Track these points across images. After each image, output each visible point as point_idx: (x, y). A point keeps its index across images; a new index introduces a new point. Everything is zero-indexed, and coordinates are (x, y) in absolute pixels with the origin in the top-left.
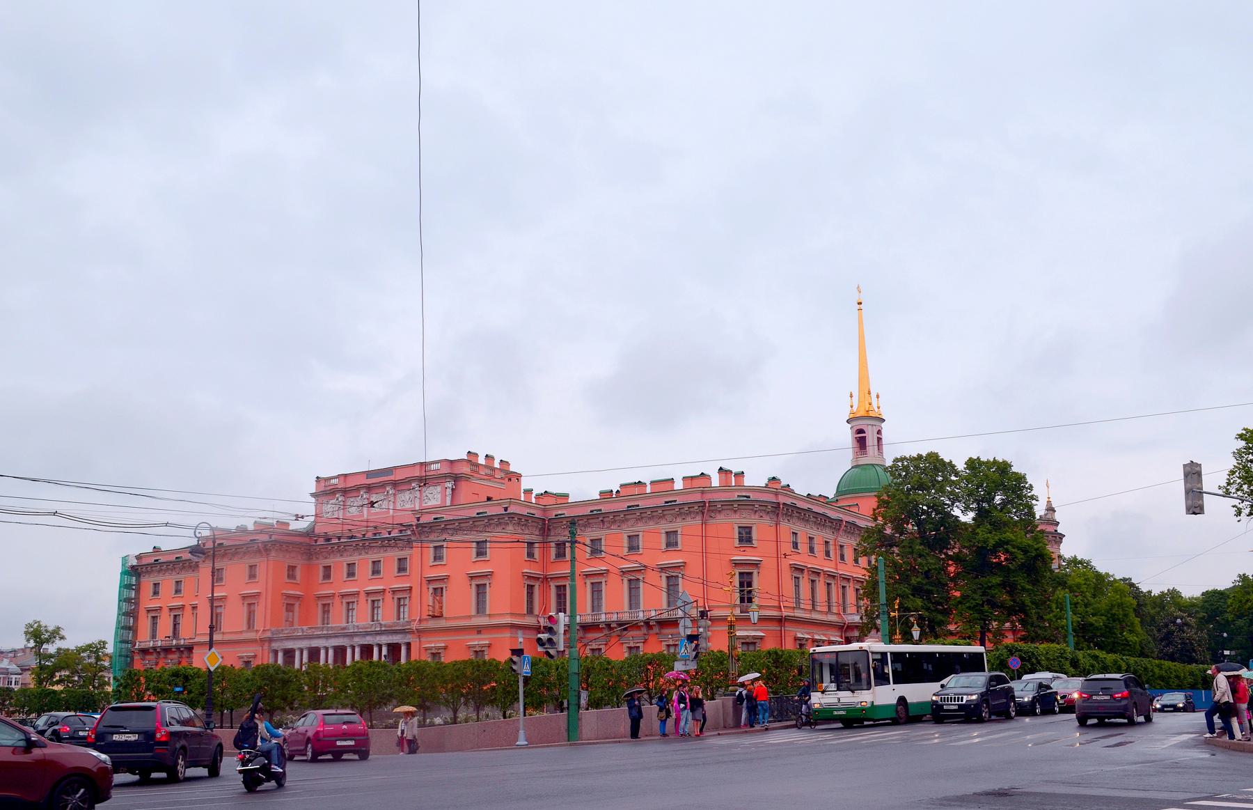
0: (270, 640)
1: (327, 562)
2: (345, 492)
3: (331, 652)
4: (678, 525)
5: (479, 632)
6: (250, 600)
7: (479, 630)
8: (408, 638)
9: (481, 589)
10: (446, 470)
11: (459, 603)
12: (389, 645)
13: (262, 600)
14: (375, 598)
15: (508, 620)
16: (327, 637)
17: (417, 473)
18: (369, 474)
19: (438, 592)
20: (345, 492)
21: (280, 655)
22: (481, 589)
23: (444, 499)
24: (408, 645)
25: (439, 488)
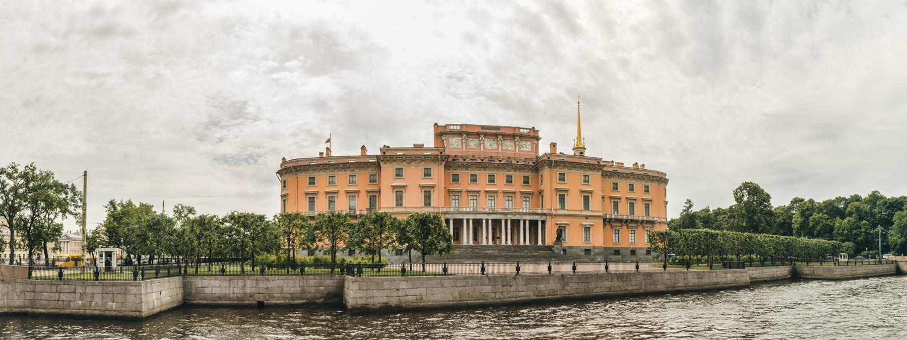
1: (456, 172)
2: (469, 134)
3: (490, 222)
7: (587, 217)
8: (544, 218)
9: (586, 199)
10: (532, 134)
11: (574, 203)
12: (530, 221)
13: (436, 189)
14: (492, 194)
15: (601, 214)
16: (488, 214)
17: (517, 132)
18: (483, 127)
20: (469, 134)
21: (451, 222)
22: (586, 199)
24: (543, 222)
25: (529, 143)
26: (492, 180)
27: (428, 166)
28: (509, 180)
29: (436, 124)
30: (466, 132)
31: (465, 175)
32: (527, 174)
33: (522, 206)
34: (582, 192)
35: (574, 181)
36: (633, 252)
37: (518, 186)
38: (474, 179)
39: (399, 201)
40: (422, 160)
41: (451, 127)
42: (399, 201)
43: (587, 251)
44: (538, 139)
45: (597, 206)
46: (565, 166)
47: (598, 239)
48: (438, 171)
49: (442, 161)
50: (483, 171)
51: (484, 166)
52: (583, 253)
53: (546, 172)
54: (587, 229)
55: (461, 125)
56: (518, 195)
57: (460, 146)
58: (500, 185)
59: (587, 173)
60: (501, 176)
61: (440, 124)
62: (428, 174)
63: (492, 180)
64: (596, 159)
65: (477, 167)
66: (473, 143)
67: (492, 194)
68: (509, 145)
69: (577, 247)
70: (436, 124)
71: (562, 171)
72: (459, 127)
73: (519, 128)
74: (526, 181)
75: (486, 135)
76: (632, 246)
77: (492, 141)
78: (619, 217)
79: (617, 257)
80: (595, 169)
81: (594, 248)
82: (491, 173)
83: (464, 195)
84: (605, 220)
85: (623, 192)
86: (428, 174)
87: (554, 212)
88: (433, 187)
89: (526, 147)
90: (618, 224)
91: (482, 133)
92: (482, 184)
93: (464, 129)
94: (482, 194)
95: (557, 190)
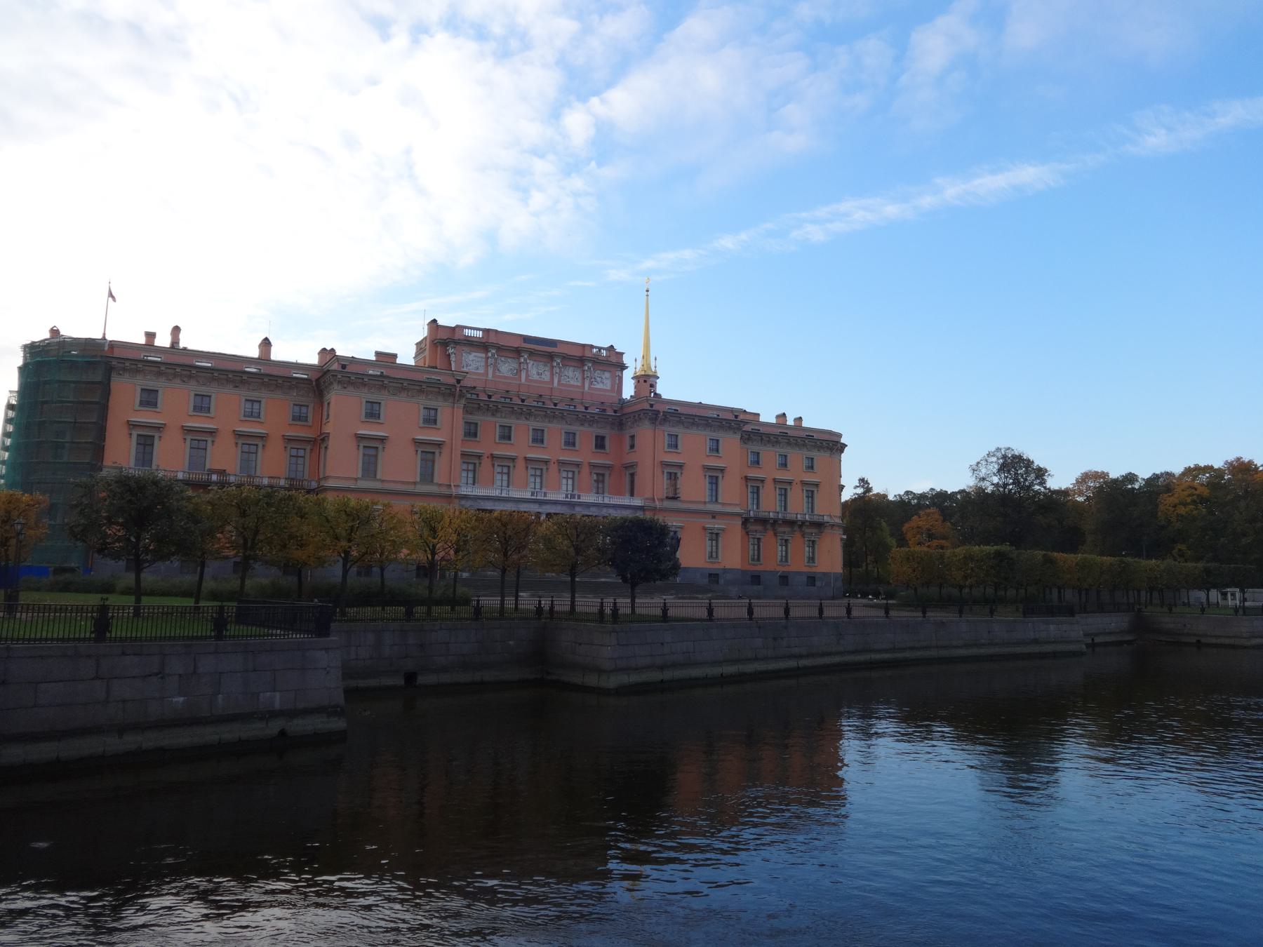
0: (466, 497)
4: (814, 454)
5: (714, 517)
6: (428, 451)
7: (714, 515)
9: (714, 482)
10: (613, 359)
11: (693, 489)
13: (446, 451)
15: (737, 510)
18: (527, 339)
19: (673, 477)
20: (500, 349)
22: (714, 482)
23: (613, 386)
25: (607, 375)
26: (538, 438)
27: (432, 404)
28: (570, 442)
29: (435, 321)
30: (494, 344)
31: (489, 425)
32: (602, 432)
33: (560, 488)
34: (707, 468)
35: (694, 445)
36: (784, 579)
37: (585, 453)
38: (506, 435)
39: (370, 468)
40: (421, 391)
41: (467, 332)
42: (370, 468)
43: (714, 577)
44: (623, 367)
45: (732, 496)
46: (680, 422)
47: (732, 556)
48: (451, 418)
49: (461, 396)
50: (522, 422)
51: (525, 412)
52: (706, 581)
53: (644, 432)
54: (715, 536)
55: (487, 331)
56: (585, 470)
57: (481, 371)
58: (554, 449)
59: (715, 435)
60: (555, 432)
61: (440, 322)
62: (431, 421)
63: (538, 438)
64: (732, 410)
65: (513, 412)
66: (506, 367)
67: (539, 466)
68: (572, 377)
69: (697, 569)
70: (435, 321)
71: (674, 430)
72: (480, 334)
73: (592, 347)
74: (600, 443)
75: (532, 354)
76: (781, 569)
77: (541, 366)
78: (761, 515)
79: (756, 588)
80: (730, 428)
81: (725, 571)
82: (538, 425)
83: (486, 462)
84: (746, 522)
85: (769, 469)
86: (431, 421)
87: (658, 504)
88: (439, 445)
89: (603, 382)
90: (759, 528)
91: (527, 350)
92: (521, 445)
93: (492, 339)
94: (520, 464)
95: (665, 465)
